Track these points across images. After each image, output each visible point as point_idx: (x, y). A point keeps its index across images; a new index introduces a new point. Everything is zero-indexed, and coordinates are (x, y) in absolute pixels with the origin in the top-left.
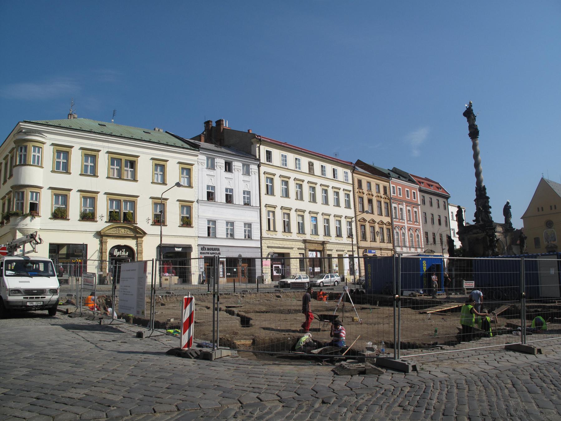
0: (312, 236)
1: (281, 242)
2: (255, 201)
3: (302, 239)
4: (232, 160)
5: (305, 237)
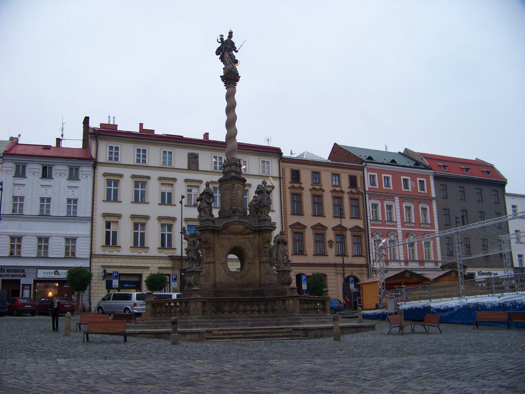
1: (127, 260)
2: (83, 210)
3: (167, 255)
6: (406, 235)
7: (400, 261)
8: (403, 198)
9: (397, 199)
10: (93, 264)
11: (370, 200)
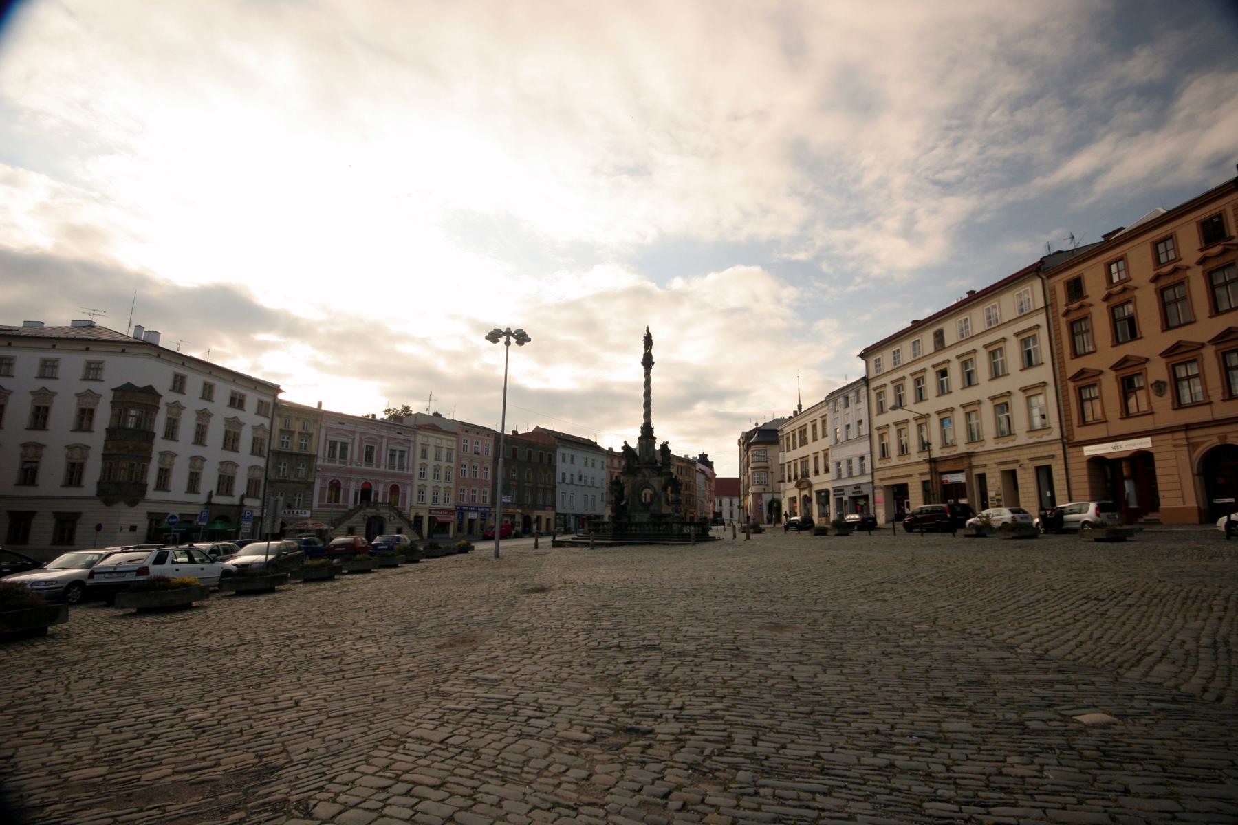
0: (969, 446)
1: (896, 470)
10: (875, 478)
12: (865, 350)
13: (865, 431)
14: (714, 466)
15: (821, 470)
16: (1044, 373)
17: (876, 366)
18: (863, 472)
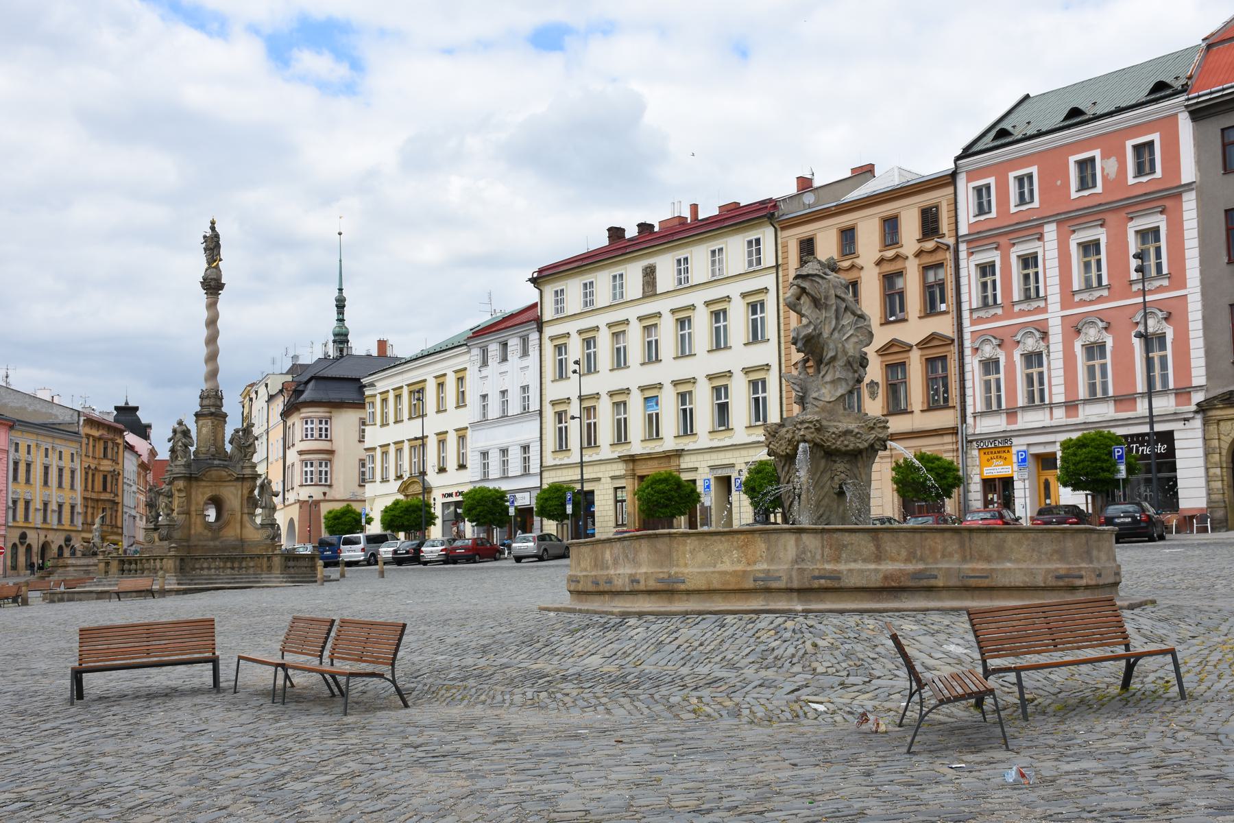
0: (679, 440)
4: (505, 338)
5: (629, 450)
6: (1074, 328)
7: (1051, 406)
8: (1069, 220)
9: (1050, 231)
11: (971, 258)
12: (540, 271)
13: (534, 407)
14: (153, 433)
15: (452, 464)
16: (767, 353)
17: (557, 302)
18: (526, 473)
